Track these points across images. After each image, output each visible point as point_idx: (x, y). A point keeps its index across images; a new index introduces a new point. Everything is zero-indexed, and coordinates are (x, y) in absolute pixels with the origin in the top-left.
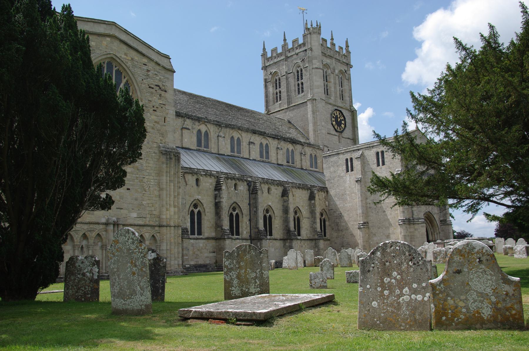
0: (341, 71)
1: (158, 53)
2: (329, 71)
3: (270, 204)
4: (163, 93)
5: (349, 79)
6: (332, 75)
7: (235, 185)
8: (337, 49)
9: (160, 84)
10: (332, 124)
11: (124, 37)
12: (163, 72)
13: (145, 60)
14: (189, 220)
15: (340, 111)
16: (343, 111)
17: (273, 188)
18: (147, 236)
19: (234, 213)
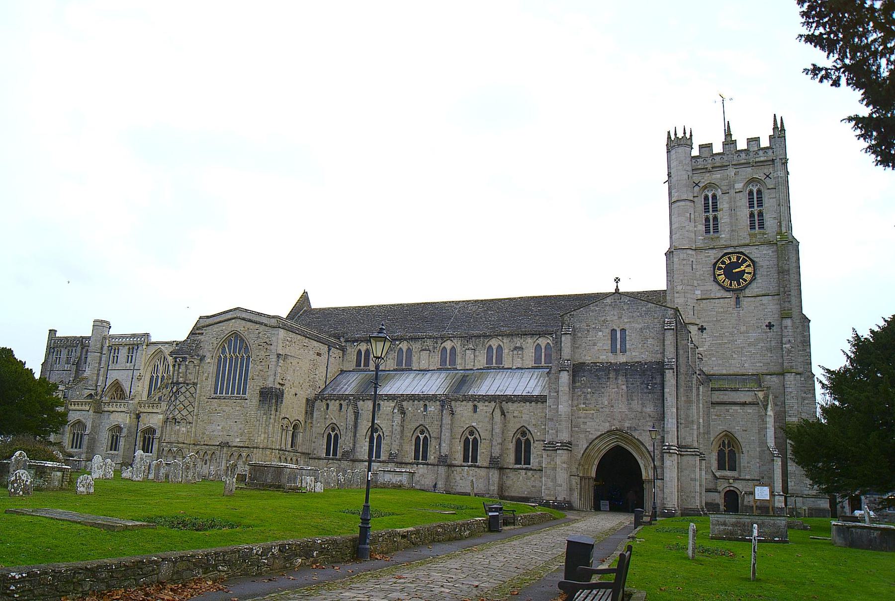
0: (752, 181)
1: (269, 316)
2: (719, 193)
3: (474, 424)
4: (268, 347)
5: (784, 184)
6: (726, 197)
7: (425, 405)
8: (742, 145)
9: (267, 340)
10: (715, 280)
11: (244, 315)
12: (270, 330)
13: (258, 326)
14: (367, 444)
16: (745, 250)
17: (480, 406)
18: (244, 454)
19: (422, 437)
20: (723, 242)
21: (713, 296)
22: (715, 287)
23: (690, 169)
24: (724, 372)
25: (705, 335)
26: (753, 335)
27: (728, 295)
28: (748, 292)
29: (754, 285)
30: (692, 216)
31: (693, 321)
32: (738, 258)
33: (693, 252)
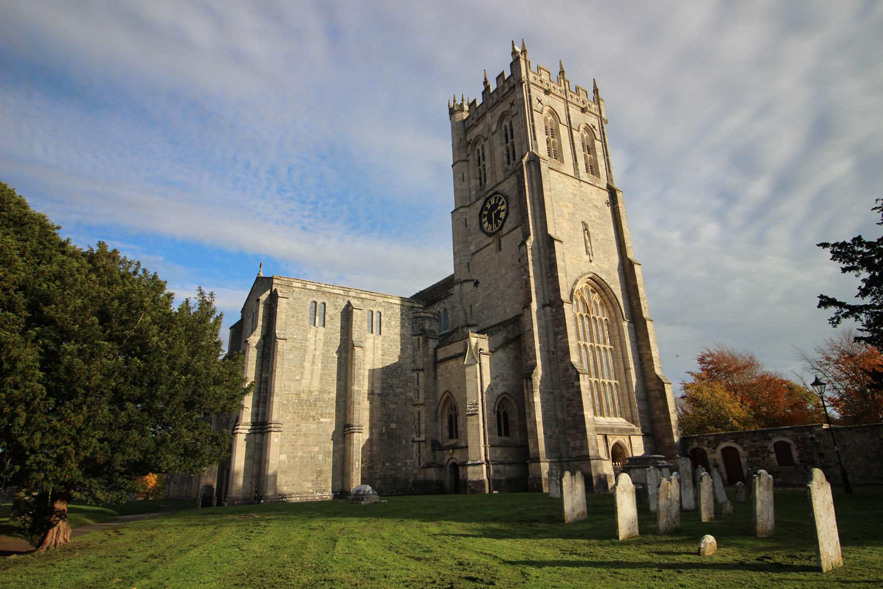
0: (503, 117)
15: (496, 193)
16: (495, 190)
20: (488, 189)
21: (482, 246)
22: (484, 236)
23: (461, 131)
24: (494, 323)
25: (479, 289)
26: (511, 275)
27: (490, 240)
28: (505, 230)
29: (508, 220)
30: (466, 175)
31: (468, 278)
32: (496, 198)
33: (467, 210)
